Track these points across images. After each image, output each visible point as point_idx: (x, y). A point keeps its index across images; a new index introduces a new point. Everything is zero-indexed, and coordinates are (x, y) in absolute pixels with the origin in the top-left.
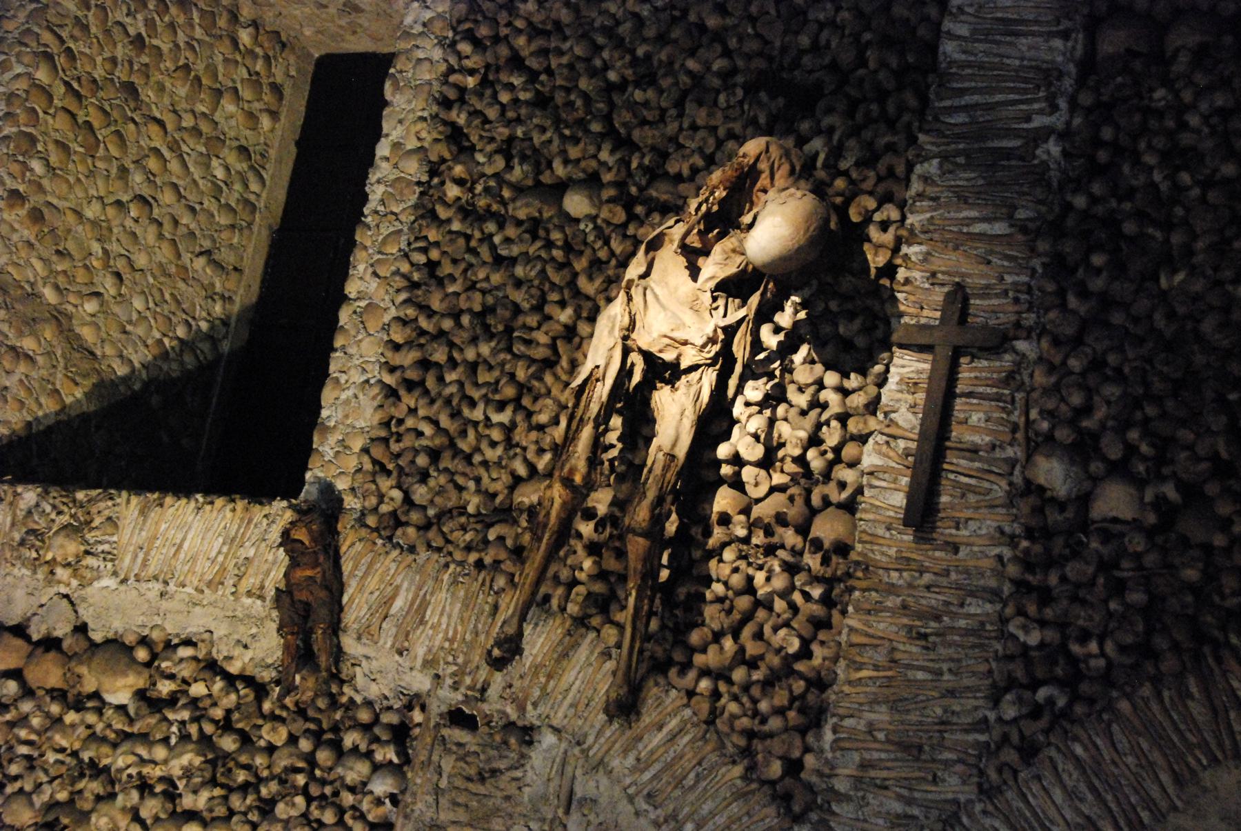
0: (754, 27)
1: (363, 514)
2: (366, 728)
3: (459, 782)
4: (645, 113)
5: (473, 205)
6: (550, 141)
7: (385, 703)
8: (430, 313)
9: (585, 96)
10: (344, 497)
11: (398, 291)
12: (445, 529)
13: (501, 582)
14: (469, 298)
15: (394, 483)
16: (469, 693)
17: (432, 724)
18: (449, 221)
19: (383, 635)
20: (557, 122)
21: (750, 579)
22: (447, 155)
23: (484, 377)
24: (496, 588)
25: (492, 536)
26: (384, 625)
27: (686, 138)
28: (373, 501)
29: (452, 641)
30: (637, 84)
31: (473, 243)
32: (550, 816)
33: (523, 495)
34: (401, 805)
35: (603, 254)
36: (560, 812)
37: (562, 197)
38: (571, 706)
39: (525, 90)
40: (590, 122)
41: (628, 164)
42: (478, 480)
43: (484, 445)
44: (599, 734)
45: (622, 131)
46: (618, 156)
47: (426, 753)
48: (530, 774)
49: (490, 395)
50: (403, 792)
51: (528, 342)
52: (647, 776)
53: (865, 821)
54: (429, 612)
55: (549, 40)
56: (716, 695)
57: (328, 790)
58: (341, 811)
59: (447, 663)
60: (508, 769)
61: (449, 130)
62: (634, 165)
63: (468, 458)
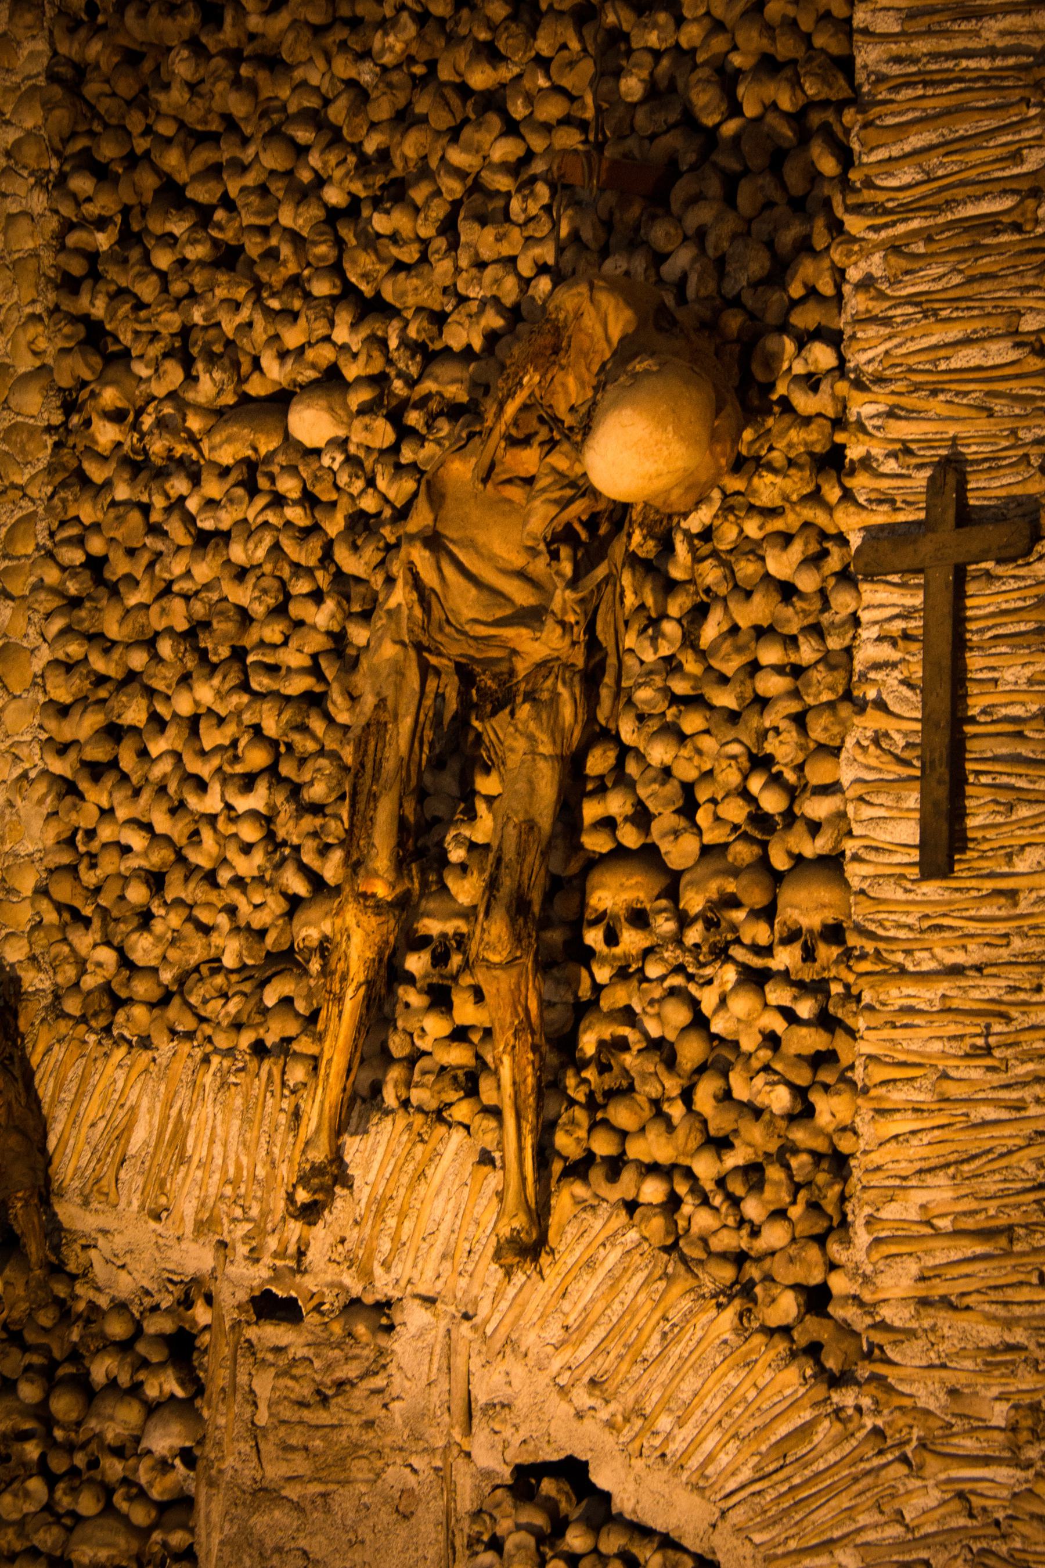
0: (548, 76)
1: (57, 997)
2: (125, 1346)
3: (287, 1412)
4: (394, 251)
5: (145, 451)
6: (250, 325)
7: (147, 1301)
8: (108, 646)
9: (295, 237)
10: (21, 973)
11: (48, 616)
12: (193, 1000)
13: (298, 1073)
14: (163, 611)
15: (98, 937)
16: (279, 1263)
17: (228, 1325)
18: (108, 484)
19: (124, 1192)
20: (258, 287)
21: (694, 1004)
22: (87, 375)
23: (211, 737)
24: (291, 1083)
25: (270, 998)
26: (122, 1174)
27: (469, 283)
28: (70, 972)
29: (234, 1183)
30: (376, 203)
31: (155, 517)
32: (441, 1443)
33: (307, 924)
34: (201, 1464)
35: (369, 504)
36: (457, 1435)
37: (285, 414)
38: (444, 1257)
39: (193, 242)
40: (309, 280)
41: (383, 342)
42: (232, 910)
43: (232, 854)
44: (497, 1296)
45: (364, 287)
46: (364, 332)
47: (226, 1373)
48: (397, 1379)
49: (228, 769)
50: (200, 1443)
51: (273, 669)
52: (586, 1349)
53: (944, 1366)
54: (190, 1142)
55: (219, 148)
56: (673, 1202)
57: (80, 1460)
58: (107, 1491)
59: (234, 1220)
60: (361, 1378)
61: (81, 331)
62: (393, 343)
63: (210, 878)
